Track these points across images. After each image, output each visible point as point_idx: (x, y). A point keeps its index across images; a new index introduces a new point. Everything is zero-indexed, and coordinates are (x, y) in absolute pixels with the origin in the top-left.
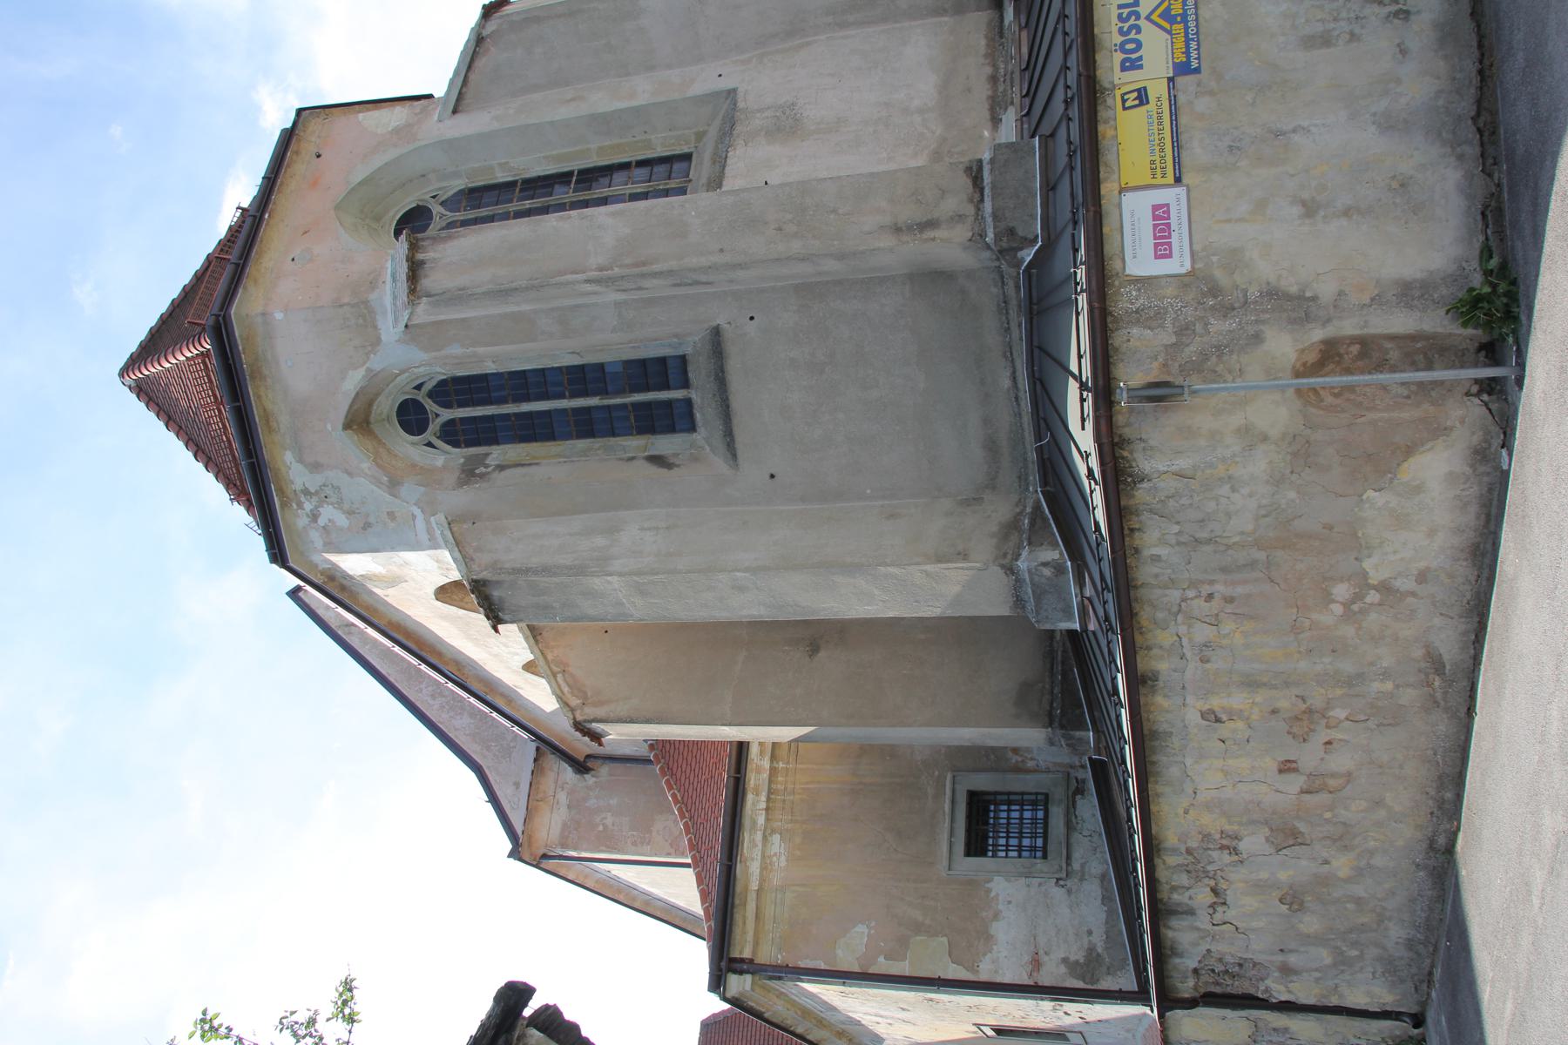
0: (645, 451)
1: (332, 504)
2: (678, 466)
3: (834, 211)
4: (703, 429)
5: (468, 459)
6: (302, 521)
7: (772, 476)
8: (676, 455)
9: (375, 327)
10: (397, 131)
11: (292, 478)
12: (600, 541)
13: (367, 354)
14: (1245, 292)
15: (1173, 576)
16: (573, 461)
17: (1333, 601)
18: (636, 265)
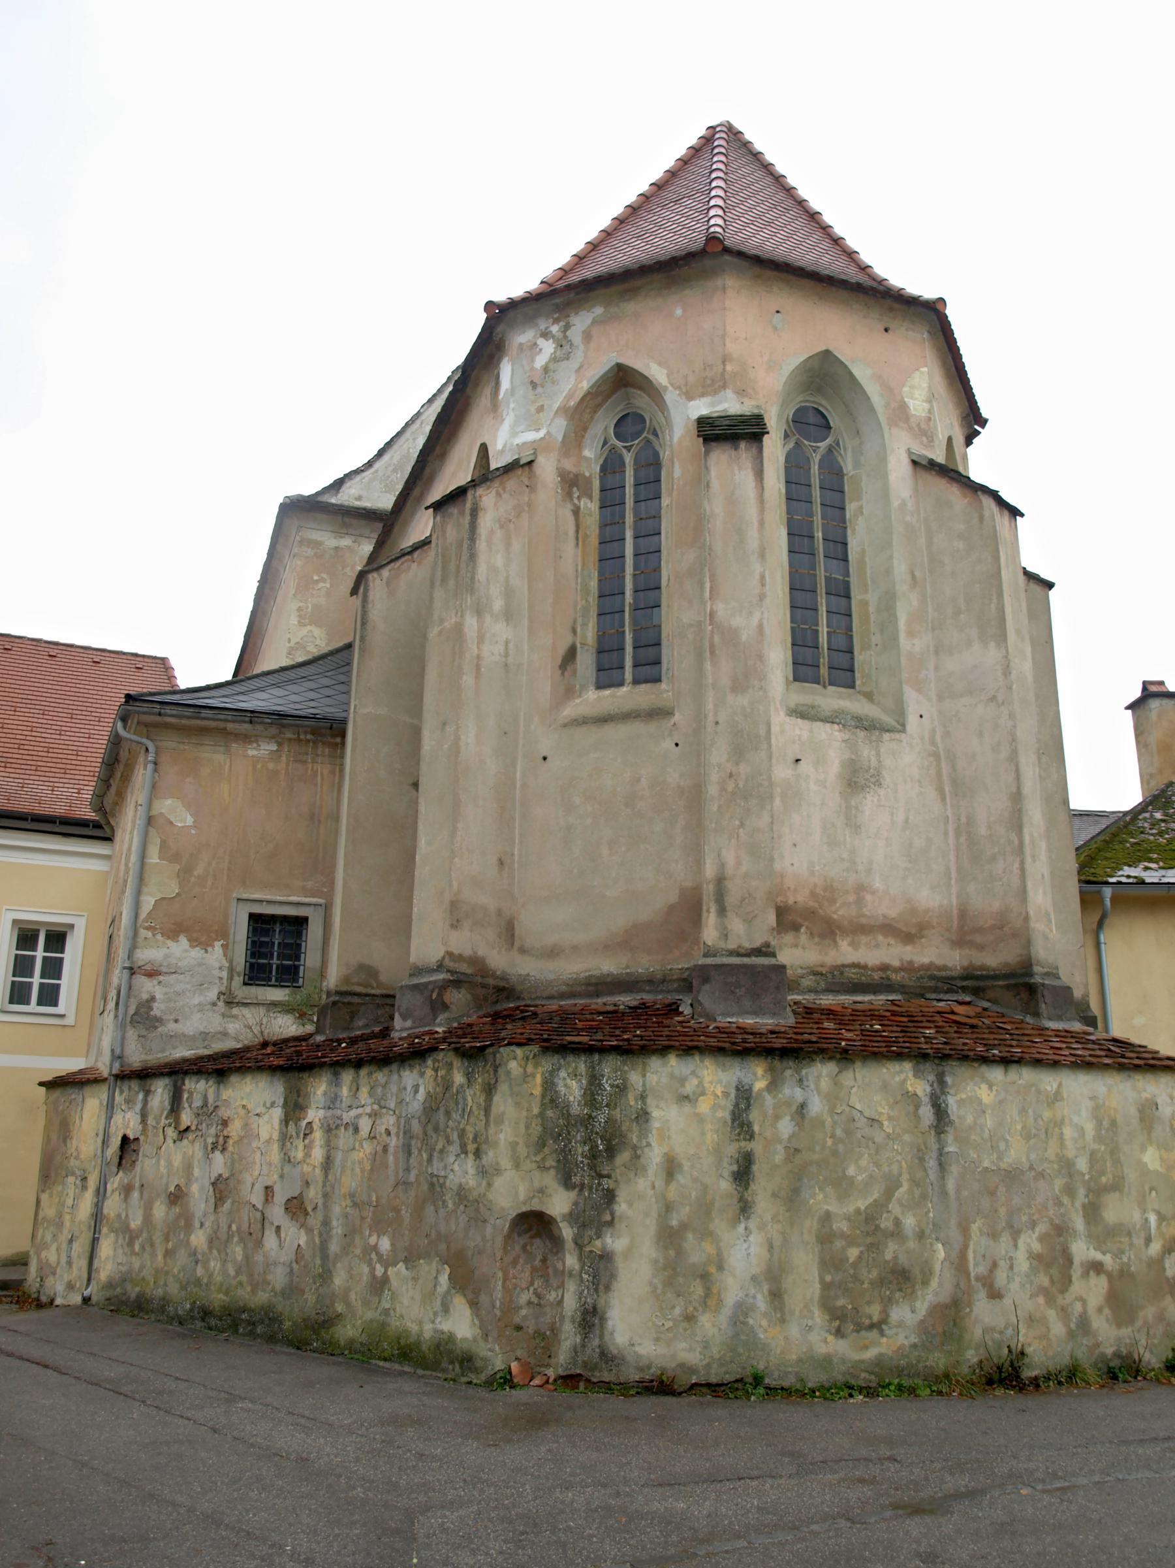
0: (581, 644)
1: (555, 352)
2: (563, 674)
3: (742, 825)
4: (596, 696)
5: (588, 481)
6: (543, 324)
7: (545, 759)
8: (575, 673)
9: (702, 395)
10: (903, 407)
11: (580, 313)
12: (498, 604)
13: (679, 388)
14: (609, 1176)
15: (404, 1102)
16: (577, 577)
17: (379, 1237)
18: (712, 646)
